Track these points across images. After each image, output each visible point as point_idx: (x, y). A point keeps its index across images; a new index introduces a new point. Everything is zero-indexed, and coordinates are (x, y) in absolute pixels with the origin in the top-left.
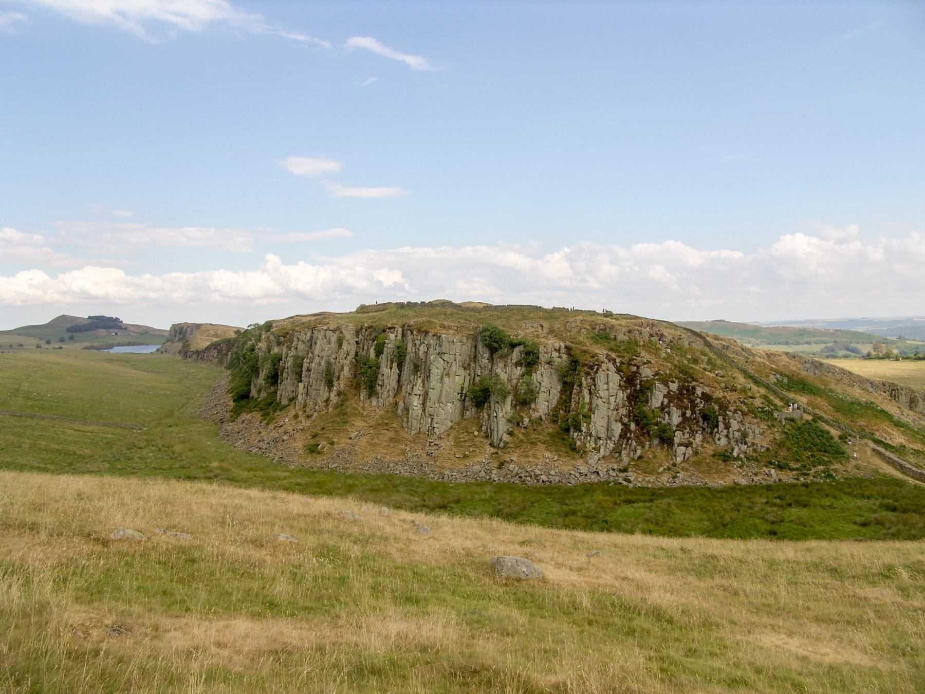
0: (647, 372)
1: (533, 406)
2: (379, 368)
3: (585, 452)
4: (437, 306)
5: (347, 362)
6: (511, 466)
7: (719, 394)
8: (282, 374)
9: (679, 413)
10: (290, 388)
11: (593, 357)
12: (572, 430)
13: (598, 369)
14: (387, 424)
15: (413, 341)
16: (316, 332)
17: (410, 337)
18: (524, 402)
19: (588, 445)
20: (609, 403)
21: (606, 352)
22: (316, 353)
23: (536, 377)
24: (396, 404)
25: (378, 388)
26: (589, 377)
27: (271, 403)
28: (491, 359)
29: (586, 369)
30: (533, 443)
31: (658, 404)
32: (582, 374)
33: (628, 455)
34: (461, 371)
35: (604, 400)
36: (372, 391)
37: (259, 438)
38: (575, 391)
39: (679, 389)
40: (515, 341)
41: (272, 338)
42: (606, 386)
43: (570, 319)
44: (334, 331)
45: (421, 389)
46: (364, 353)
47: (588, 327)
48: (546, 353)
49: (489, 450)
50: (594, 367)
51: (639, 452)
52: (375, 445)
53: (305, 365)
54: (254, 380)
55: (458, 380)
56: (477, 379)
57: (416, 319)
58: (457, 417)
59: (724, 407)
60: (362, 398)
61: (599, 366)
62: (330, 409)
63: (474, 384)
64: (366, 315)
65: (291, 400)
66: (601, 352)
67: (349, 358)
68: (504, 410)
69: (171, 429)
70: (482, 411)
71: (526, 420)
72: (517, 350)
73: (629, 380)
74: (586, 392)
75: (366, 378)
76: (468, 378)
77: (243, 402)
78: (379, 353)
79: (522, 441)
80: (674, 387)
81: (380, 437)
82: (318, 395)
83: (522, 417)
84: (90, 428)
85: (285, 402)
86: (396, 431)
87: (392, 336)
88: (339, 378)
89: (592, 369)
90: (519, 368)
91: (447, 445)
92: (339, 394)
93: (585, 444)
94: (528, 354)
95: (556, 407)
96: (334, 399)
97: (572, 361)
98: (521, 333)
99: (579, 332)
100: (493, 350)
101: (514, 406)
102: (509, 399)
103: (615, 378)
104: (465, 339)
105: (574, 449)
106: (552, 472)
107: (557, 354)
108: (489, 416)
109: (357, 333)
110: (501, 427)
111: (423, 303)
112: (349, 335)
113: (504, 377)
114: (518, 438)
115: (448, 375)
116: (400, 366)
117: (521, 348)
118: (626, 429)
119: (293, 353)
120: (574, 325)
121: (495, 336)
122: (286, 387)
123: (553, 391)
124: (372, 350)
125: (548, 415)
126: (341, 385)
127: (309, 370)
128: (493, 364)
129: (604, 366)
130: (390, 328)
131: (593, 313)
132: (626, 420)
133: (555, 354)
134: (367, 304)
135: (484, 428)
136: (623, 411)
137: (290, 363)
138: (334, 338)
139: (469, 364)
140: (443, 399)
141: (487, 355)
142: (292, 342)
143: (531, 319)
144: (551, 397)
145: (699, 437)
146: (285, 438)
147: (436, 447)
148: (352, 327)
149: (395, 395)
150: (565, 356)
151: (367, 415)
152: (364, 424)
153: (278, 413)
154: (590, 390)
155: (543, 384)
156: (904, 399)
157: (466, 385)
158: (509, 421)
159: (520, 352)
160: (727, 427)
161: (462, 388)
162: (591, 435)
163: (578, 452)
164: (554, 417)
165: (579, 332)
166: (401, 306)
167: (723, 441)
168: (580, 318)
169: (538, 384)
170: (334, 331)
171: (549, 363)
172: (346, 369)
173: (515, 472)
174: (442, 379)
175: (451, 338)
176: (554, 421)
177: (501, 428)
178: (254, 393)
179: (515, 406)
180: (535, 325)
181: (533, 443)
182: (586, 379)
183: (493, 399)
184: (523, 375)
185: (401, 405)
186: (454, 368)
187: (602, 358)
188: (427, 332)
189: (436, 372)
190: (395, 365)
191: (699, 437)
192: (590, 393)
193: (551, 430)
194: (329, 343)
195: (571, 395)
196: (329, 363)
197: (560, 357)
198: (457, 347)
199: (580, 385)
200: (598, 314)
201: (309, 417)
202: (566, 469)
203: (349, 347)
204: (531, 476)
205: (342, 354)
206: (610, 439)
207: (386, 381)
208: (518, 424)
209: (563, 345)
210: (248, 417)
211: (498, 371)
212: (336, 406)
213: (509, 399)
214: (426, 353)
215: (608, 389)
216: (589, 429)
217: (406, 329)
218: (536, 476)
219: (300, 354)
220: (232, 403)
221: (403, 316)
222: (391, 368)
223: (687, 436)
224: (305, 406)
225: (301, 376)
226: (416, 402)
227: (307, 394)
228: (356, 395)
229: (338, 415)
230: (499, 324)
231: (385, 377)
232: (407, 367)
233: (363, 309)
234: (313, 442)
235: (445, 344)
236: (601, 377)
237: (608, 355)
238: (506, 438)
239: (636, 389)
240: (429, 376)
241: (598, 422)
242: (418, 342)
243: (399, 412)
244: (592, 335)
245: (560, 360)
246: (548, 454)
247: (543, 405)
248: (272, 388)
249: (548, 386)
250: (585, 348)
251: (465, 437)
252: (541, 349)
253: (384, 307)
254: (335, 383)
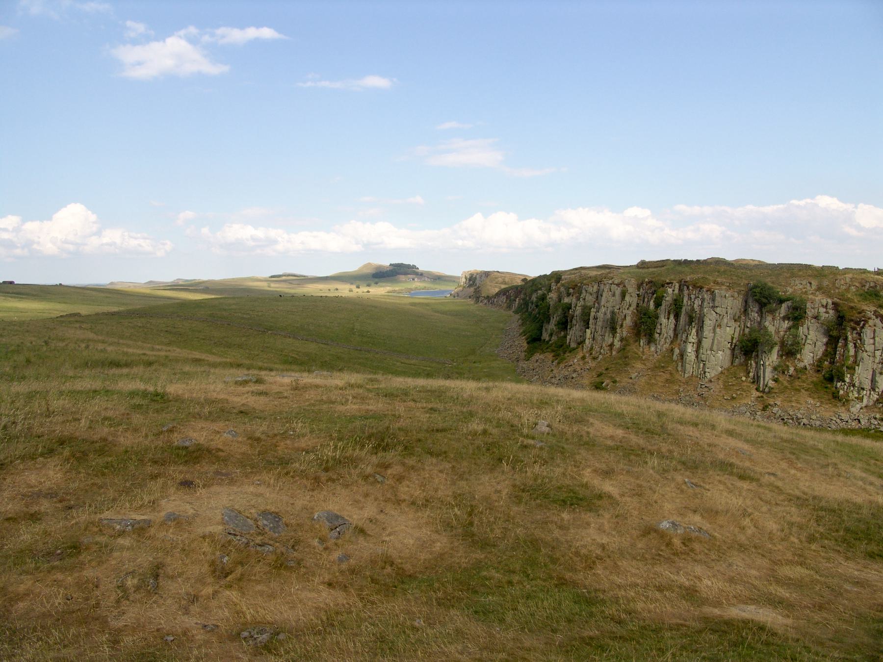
1: (798, 356)
2: (657, 318)
3: (847, 401)
4: (711, 263)
5: (629, 312)
6: (775, 409)
8: (571, 321)
10: (579, 333)
11: (860, 313)
12: (835, 380)
13: (864, 325)
14: (663, 367)
15: (689, 295)
16: (602, 286)
17: (686, 292)
18: (790, 351)
19: (850, 395)
20: (874, 356)
21: (873, 309)
22: (602, 304)
24: (672, 350)
25: (657, 335)
26: (855, 332)
27: (562, 346)
28: (761, 313)
29: (852, 324)
30: (796, 390)
32: (849, 329)
34: (732, 323)
35: (869, 354)
36: (651, 340)
37: (552, 375)
38: (840, 344)
40: (784, 297)
41: (562, 289)
42: (872, 341)
43: (839, 277)
44: (618, 285)
45: (695, 337)
46: (645, 305)
47: (857, 285)
48: (813, 308)
49: (755, 394)
52: (652, 385)
53: (592, 314)
54: (545, 326)
55: (729, 332)
56: (747, 330)
57: (692, 276)
58: (727, 364)
60: (642, 344)
61: (866, 322)
62: (614, 353)
63: (744, 335)
64: (646, 270)
65: (579, 344)
66: (869, 309)
67: (631, 308)
68: (773, 358)
69: (476, 365)
70: (750, 359)
71: (792, 369)
72: (784, 305)
74: (851, 346)
75: (645, 326)
76: (738, 329)
77: (536, 344)
78: (658, 305)
79: (786, 387)
81: (658, 378)
82: (603, 340)
83: (788, 366)
84: (413, 362)
85: (573, 345)
86: (671, 374)
87: (670, 290)
88: (622, 326)
89: (859, 325)
90: (786, 322)
91: (716, 387)
92: (622, 340)
93: (848, 393)
94: (795, 309)
95: (821, 358)
96: (617, 344)
97: (839, 317)
98: (790, 290)
99: (847, 290)
100: (762, 306)
102: (776, 349)
104: (736, 295)
105: (836, 396)
106: (814, 417)
107: (824, 310)
108: (756, 363)
109: (639, 287)
110: (767, 374)
111: (698, 261)
112: (631, 289)
113: (771, 329)
114: (782, 384)
115: (720, 326)
116: (677, 316)
117: (789, 303)
119: (581, 303)
120: (842, 282)
121: (763, 291)
122: (573, 334)
123: (819, 344)
124: (652, 303)
125: (813, 365)
126: (624, 331)
127: (595, 318)
128: (762, 317)
129: (871, 322)
130: (668, 284)
131: (864, 271)
133: (822, 310)
134: (647, 260)
135: (751, 374)
137: (578, 311)
138: (618, 291)
139: (739, 317)
140: (715, 348)
141: (756, 309)
142: (581, 293)
143: (800, 276)
144: (816, 349)
146: (574, 375)
147: (706, 389)
148: (633, 281)
149: (672, 342)
150: (831, 312)
151: (647, 359)
152: (643, 366)
153: (567, 354)
154: (855, 344)
155: (809, 337)
157: (736, 335)
158: (775, 369)
159: (788, 307)
161: (732, 338)
162: (854, 386)
163: (840, 401)
164: (818, 367)
165: (847, 290)
166: (678, 263)
168: (850, 275)
169: (804, 337)
170: (618, 285)
171: (816, 318)
172: (628, 319)
173: (778, 415)
174: (714, 329)
175: (723, 293)
176: (819, 371)
177: (768, 375)
178: (545, 336)
179: (782, 356)
180: (804, 282)
181: (796, 390)
182: (852, 334)
183: (759, 348)
184: (790, 328)
185: (677, 351)
186: (725, 320)
187: (870, 314)
188: (701, 288)
189: (708, 323)
190: (672, 317)
192: (855, 347)
193: (815, 379)
194: (614, 295)
195: (836, 347)
196: (613, 313)
197: (827, 312)
198: (730, 302)
199: (846, 339)
200: (869, 272)
201: (594, 358)
202: (827, 415)
203: (632, 299)
204: (792, 419)
205: (626, 305)
206: (874, 390)
207: (664, 330)
208: (783, 373)
209: (830, 301)
210: (542, 357)
211: (767, 324)
212: (619, 351)
213: (776, 349)
214: (701, 306)
215: (874, 344)
216: (852, 379)
217: (683, 284)
218: (798, 419)
219: (589, 304)
220: (525, 344)
221: (681, 273)
222: (668, 319)
224: (592, 349)
225: (588, 324)
226: (690, 349)
227: (594, 339)
228: (636, 341)
229: (620, 358)
230: (769, 281)
231: (663, 327)
232: (683, 318)
233: (643, 265)
234: (598, 380)
235: (718, 299)
236: (867, 333)
237: (875, 312)
238: (771, 384)
240: (702, 327)
242: (693, 297)
243: (675, 358)
244: (862, 292)
245: (827, 315)
246: (810, 401)
248: (563, 333)
249: (814, 339)
250: (852, 305)
251: (732, 381)
252: (809, 305)
253: (663, 263)
254: (618, 330)
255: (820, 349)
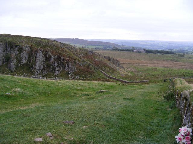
0: (49, 53)
7: (67, 59)
9: (57, 63)
23: (22, 54)
28: (11, 49)
31: (52, 61)
33: (45, 73)
34: (3, 52)
39: (57, 57)
50: (36, 52)
51: (47, 72)
59: (67, 62)
66: (39, 48)
73: (45, 55)
80: (56, 57)
100: (11, 47)
101: (16, 61)
102: (15, 60)
103: (42, 54)
105: (31, 72)
117: (19, 47)
118: (44, 67)
132: (44, 65)
133: (27, 48)
135: (9, 67)
136: (44, 62)
139: (5, 50)
141: (9, 48)
145: (61, 69)
150: (30, 49)
156: (111, 60)
157: (4, 56)
160: (68, 66)
167: (67, 70)
191: (61, 69)
223: (59, 68)
236: (38, 55)
239: (47, 58)
241: (38, 64)
247: (24, 62)
255: (27, 58)
